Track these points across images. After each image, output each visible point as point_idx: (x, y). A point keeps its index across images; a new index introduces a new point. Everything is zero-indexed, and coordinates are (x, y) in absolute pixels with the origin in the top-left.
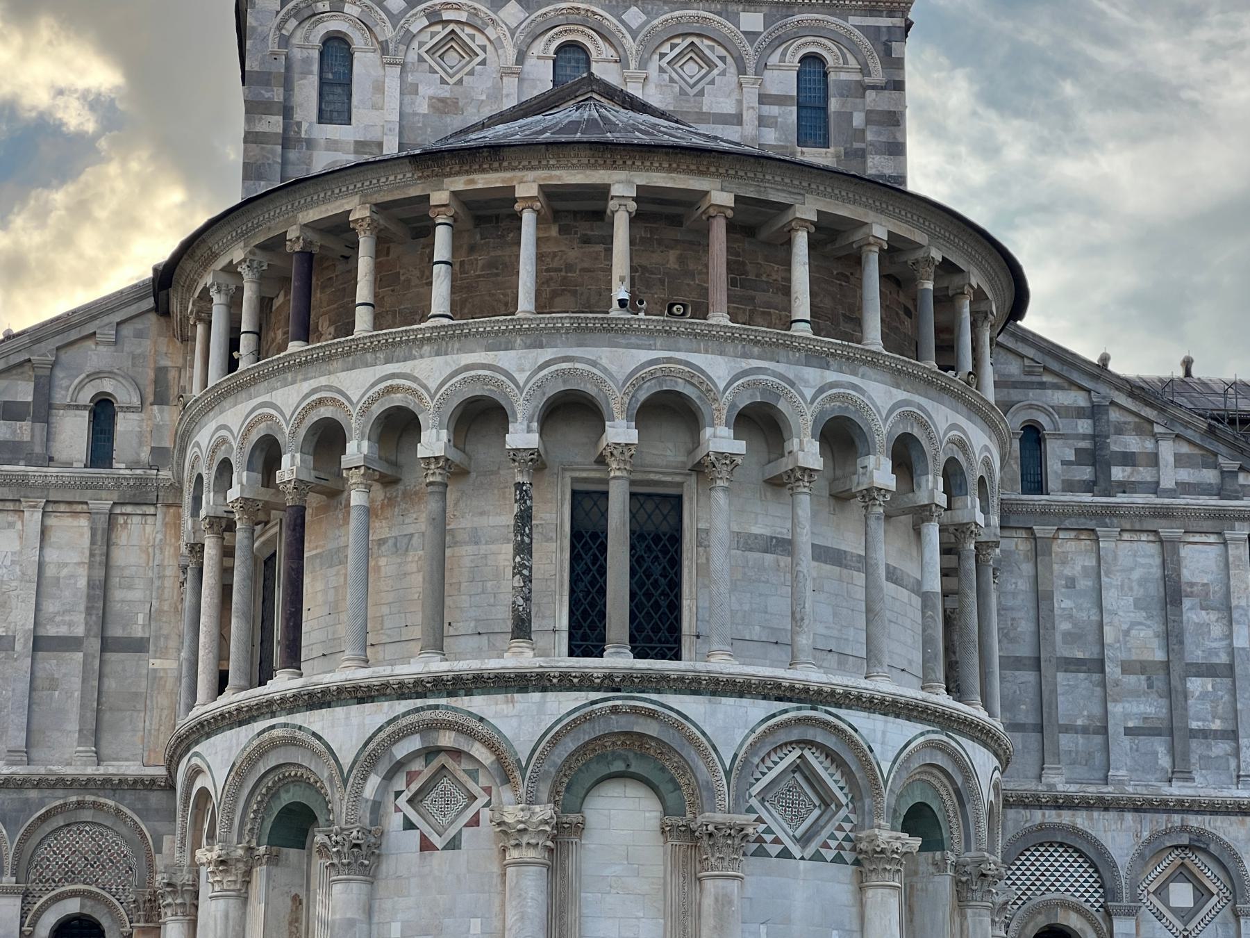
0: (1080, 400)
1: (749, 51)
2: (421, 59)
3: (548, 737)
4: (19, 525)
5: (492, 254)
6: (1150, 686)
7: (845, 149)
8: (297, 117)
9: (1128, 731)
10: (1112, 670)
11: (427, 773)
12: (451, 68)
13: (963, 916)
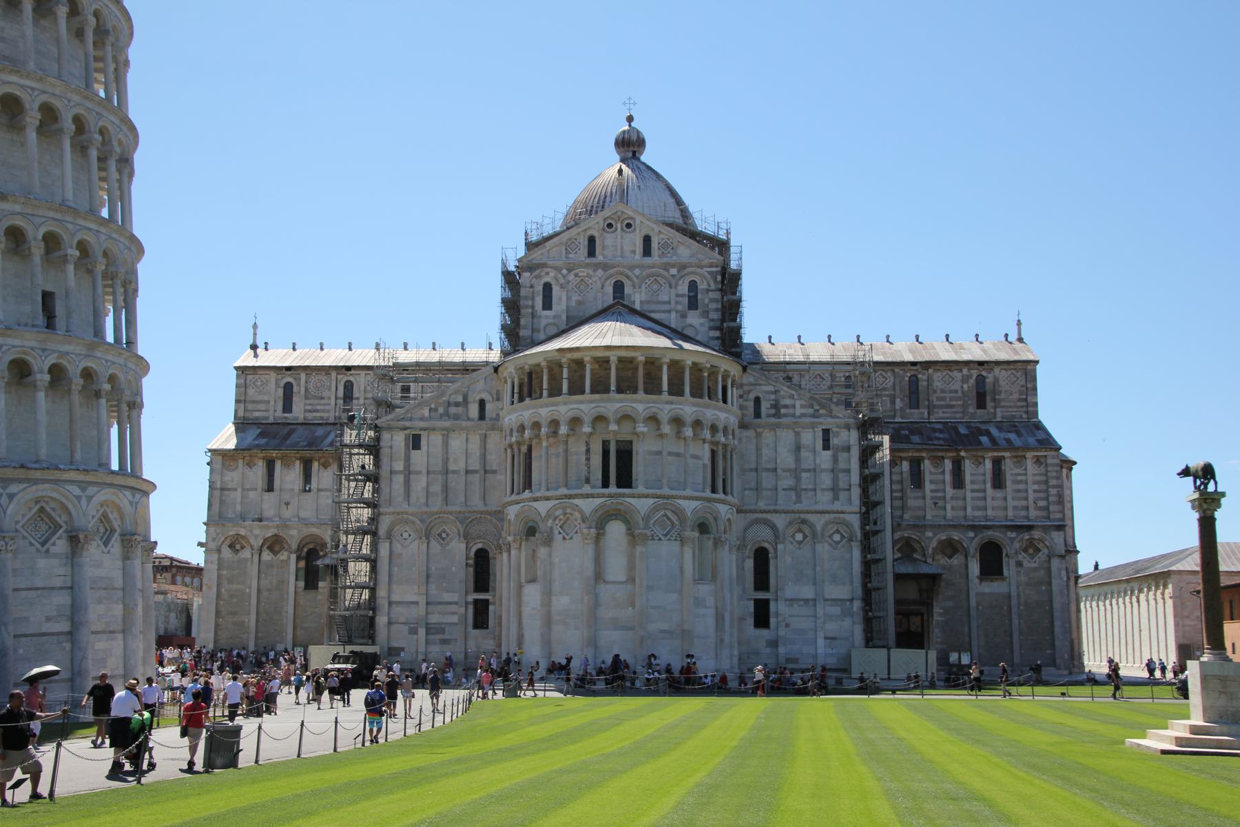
0: (771, 388)
1: (673, 281)
8: (536, 309)
10: (779, 471)
11: (564, 519)
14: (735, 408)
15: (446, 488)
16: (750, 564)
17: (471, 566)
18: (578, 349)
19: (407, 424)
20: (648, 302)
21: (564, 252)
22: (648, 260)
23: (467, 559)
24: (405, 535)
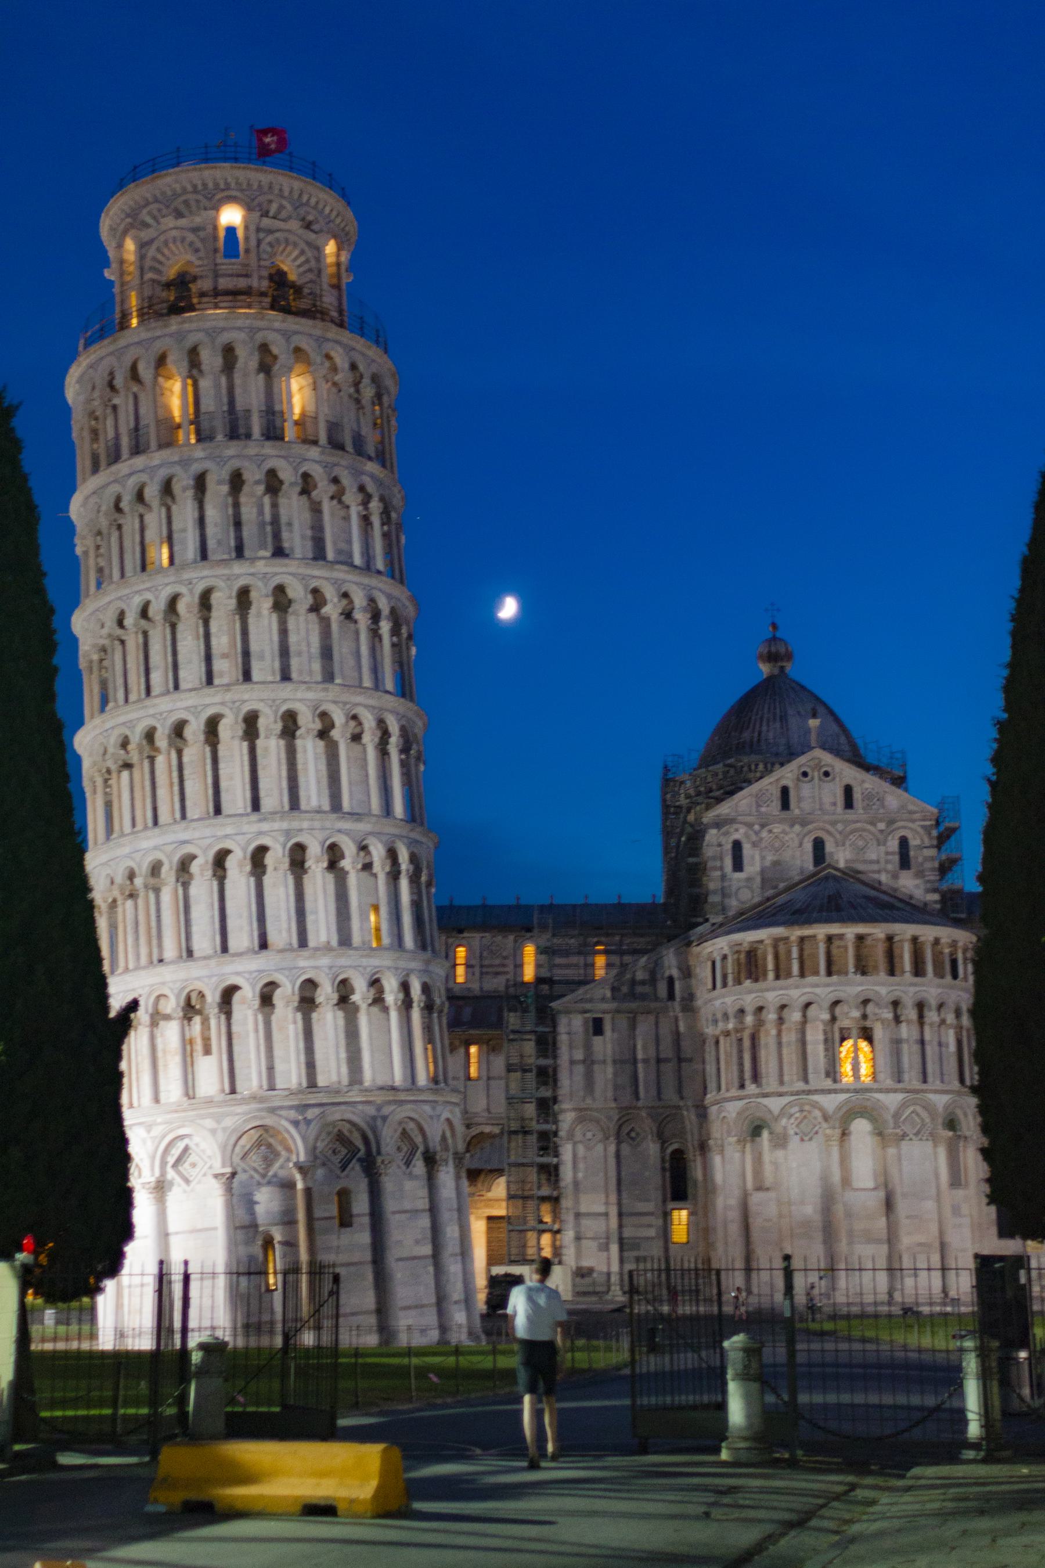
1: (881, 837)
19: (588, 1006)
20: (853, 861)
21: (754, 806)
22: (850, 815)
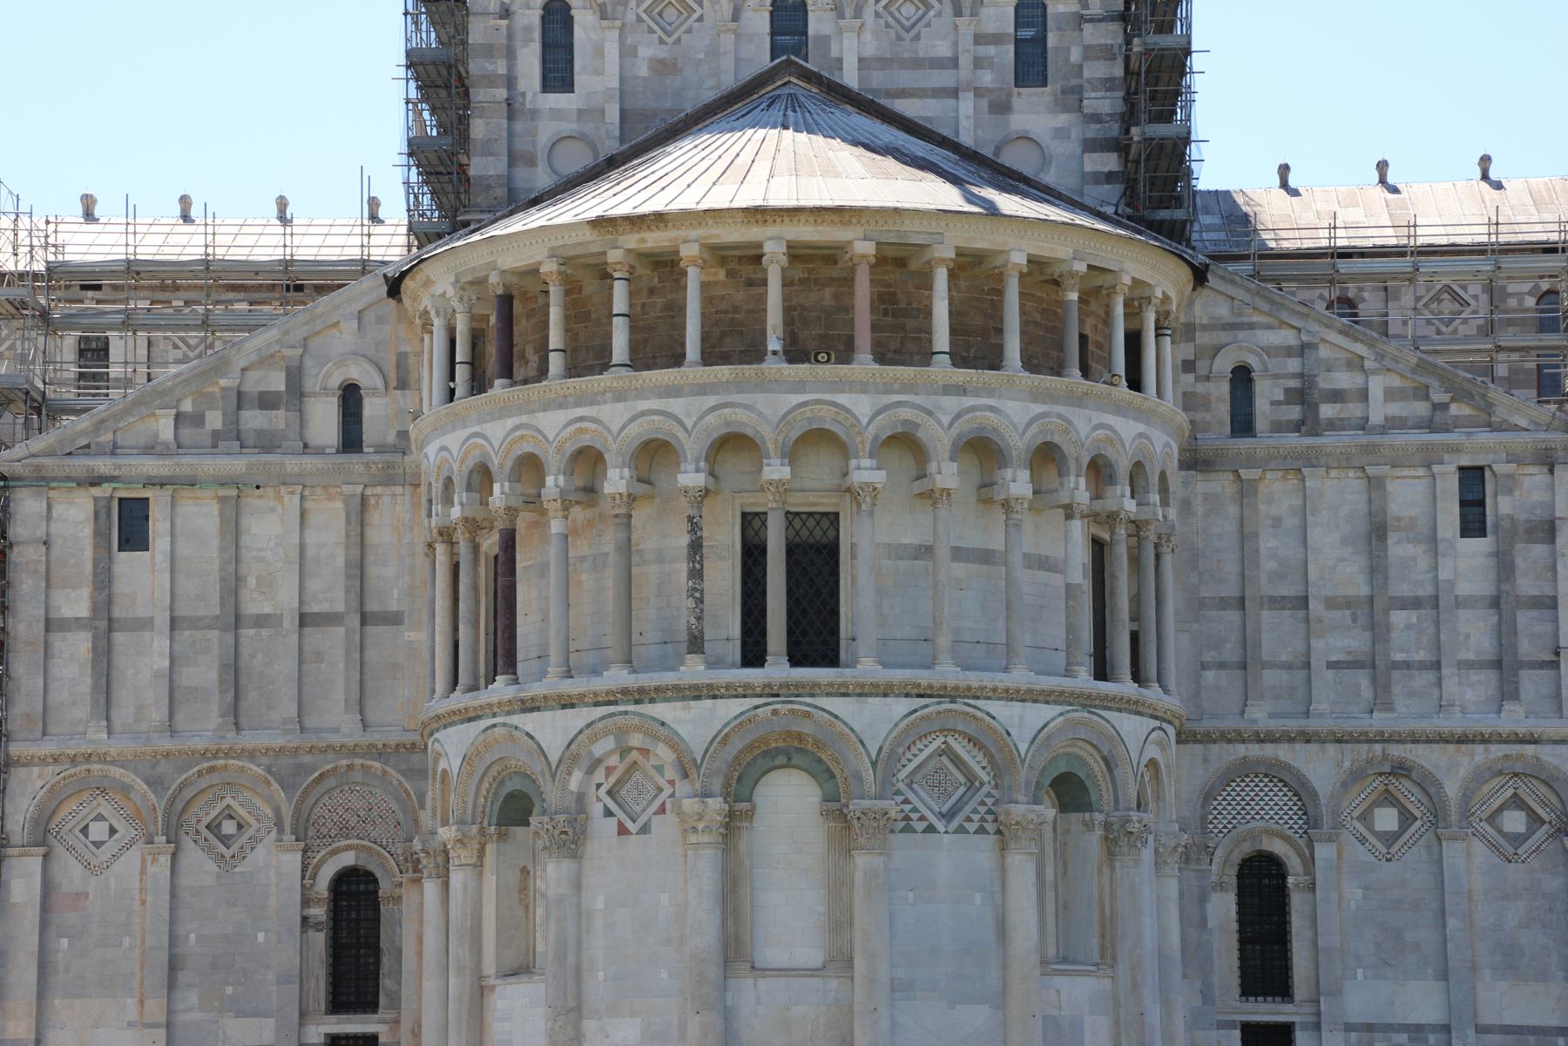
0: (1287, 337)
2: (639, 19)
3: (719, 738)
4: (280, 509)
5: (669, 297)
6: (1354, 620)
7: (1062, 87)
8: (522, 86)
9: (1332, 665)
12: (670, 24)
13: (1112, 868)
14: (1169, 403)
15: (234, 673)
16: (1224, 908)
17: (317, 926)
18: (659, 219)
19: (103, 465)
20: (884, 62)
23: (306, 902)
24: (98, 831)
